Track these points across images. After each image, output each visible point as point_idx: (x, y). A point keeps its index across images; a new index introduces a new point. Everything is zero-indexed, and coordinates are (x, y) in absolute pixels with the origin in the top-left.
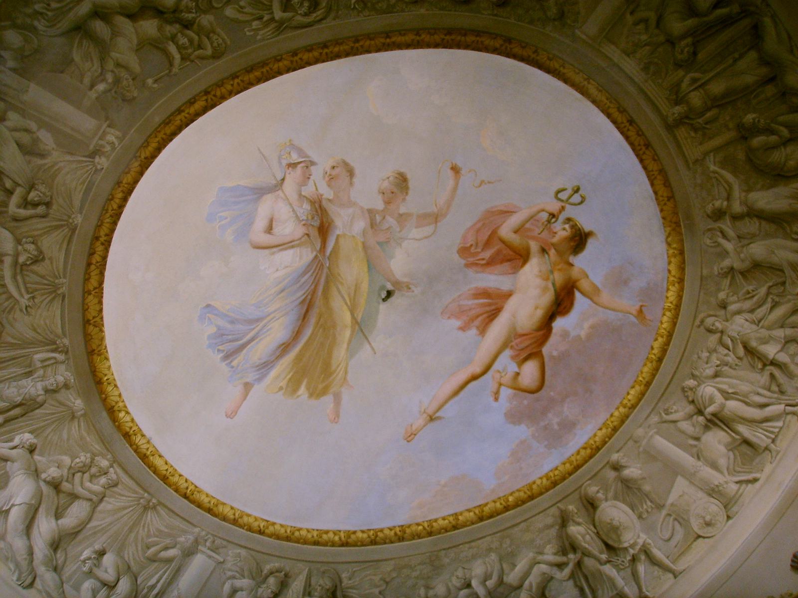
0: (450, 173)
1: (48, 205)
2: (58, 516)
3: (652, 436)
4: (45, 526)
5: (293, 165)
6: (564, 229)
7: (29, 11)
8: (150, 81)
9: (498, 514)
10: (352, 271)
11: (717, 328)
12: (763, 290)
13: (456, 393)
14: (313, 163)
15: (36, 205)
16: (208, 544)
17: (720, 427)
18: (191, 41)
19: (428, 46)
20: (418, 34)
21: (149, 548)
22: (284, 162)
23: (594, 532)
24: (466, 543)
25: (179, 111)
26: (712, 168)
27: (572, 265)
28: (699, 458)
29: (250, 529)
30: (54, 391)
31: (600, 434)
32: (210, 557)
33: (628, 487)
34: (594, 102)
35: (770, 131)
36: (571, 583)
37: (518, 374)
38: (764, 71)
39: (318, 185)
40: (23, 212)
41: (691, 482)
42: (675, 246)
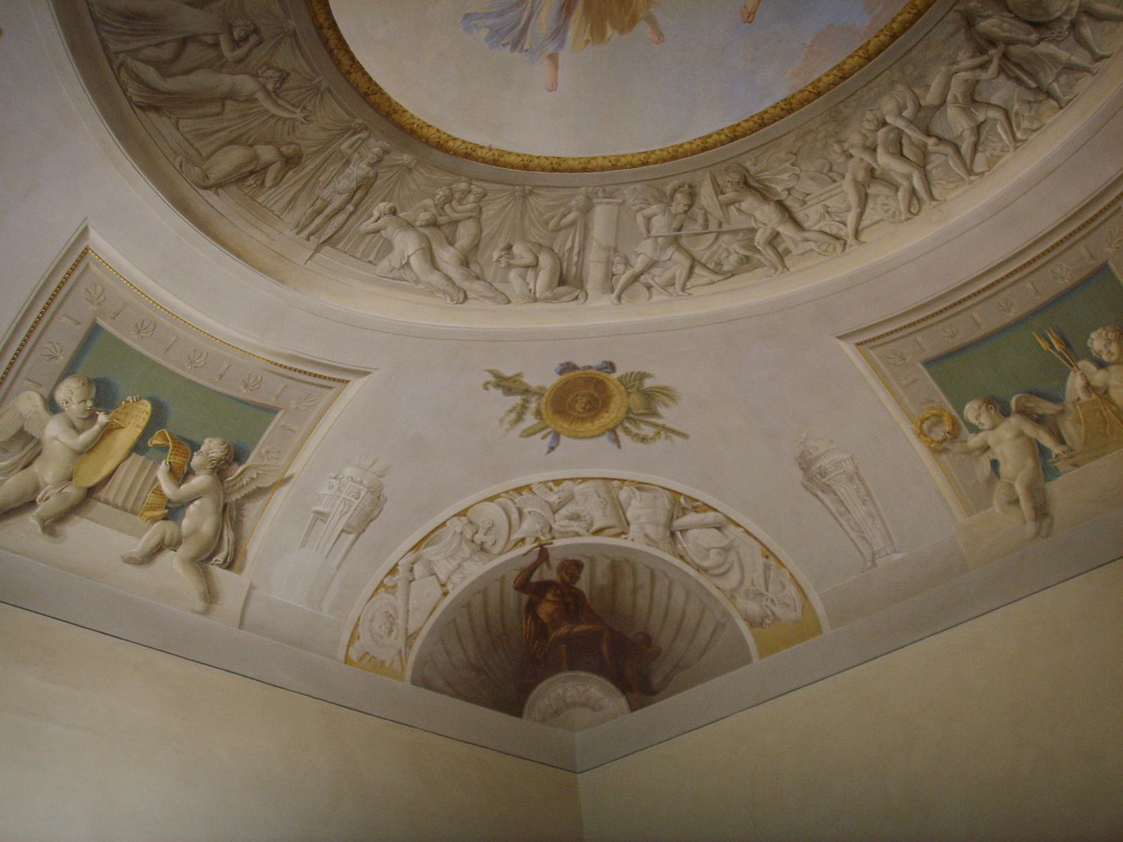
1: (256, 31)
2: (452, 243)
4: (447, 256)
9: (886, 47)
15: (245, 39)
16: (600, 194)
21: (547, 224)
23: (1012, 18)
24: (864, 86)
30: (379, 161)
32: (608, 203)
36: (1002, 78)
40: (240, 52)
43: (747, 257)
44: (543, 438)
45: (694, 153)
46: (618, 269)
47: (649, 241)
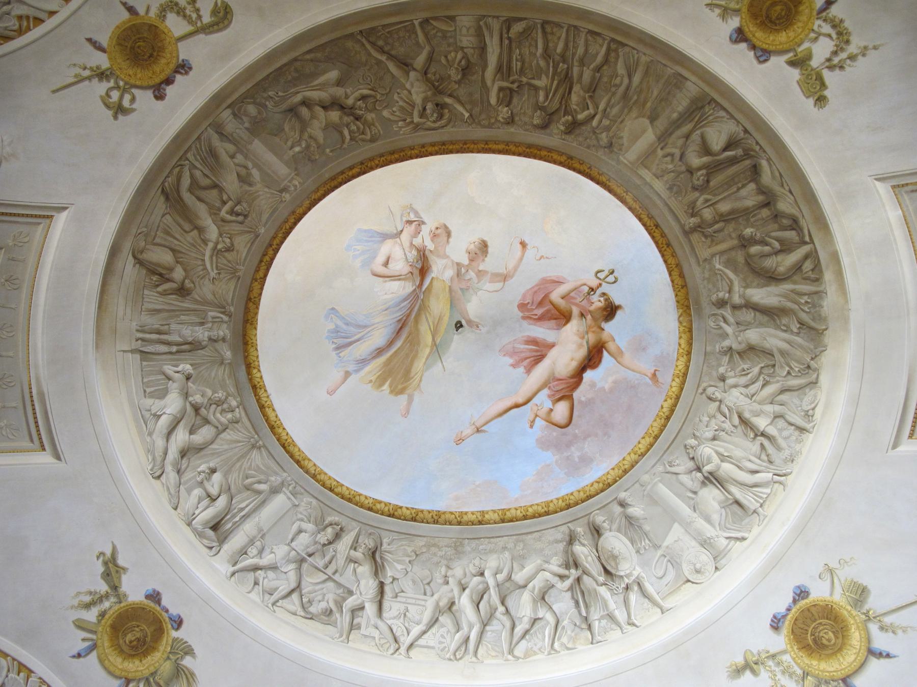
0: (519, 247)
1: (246, 216)
2: (192, 432)
3: (655, 484)
4: (181, 437)
5: (410, 222)
7: (265, 95)
8: (328, 150)
10: (438, 306)
12: (756, 370)
13: (501, 414)
14: (423, 223)
15: (238, 215)
16: (290, 488)
18: (358, 128)
19: (514, 154)
20: (507, 145)
21: (247, 478)
22: (405, 219)
25: (342, 173)
27: (603, 330)
28: (695, 511)
29: (324, 485)
30: (215, 341)
32: (289, 498)
34: (630, 209)
35: (763, 243)
36: (569, 594)
37: (551, 410)
38: (761, 198)
39: (425, 239)
40: (229, 217)
43: (331, 611)
44: (83, 640)
45: (362, 507)
46: (253, 551)
47: (287, 548)
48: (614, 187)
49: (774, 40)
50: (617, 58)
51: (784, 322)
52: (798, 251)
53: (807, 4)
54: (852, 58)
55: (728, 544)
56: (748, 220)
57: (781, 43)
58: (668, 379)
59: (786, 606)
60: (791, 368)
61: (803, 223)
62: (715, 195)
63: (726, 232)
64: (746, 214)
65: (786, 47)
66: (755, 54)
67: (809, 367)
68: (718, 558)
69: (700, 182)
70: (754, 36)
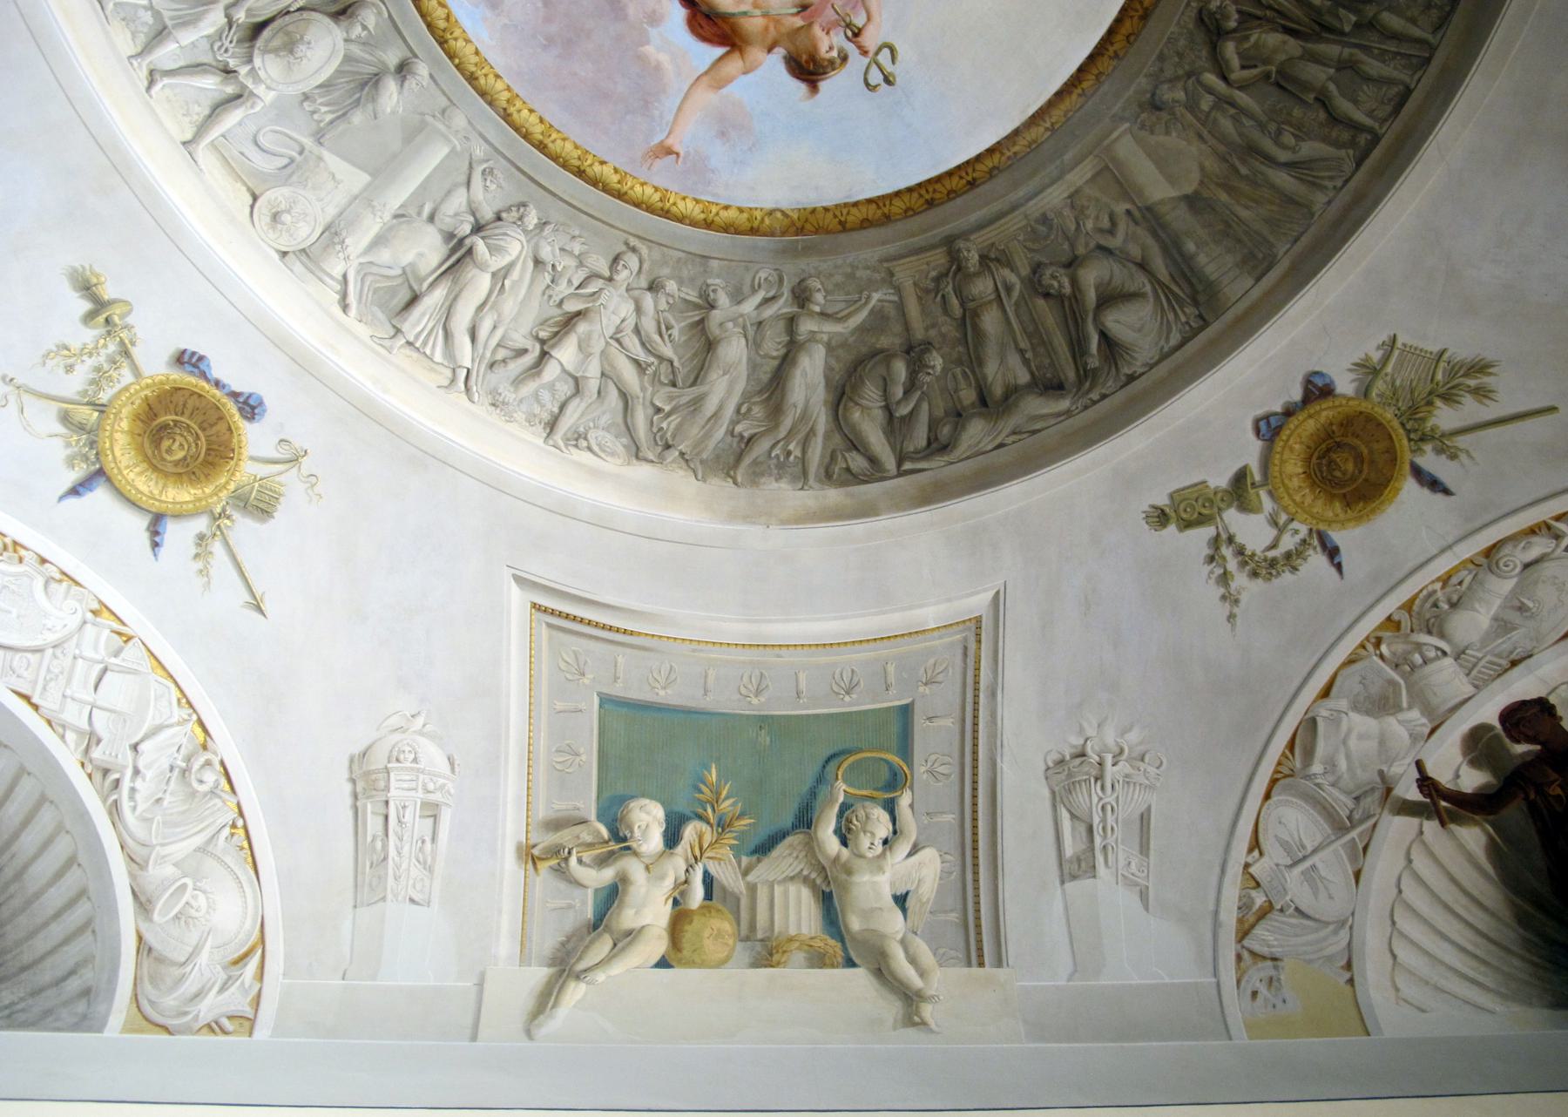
6: (831, 48)
11: (617, 272)
12: (667, 351)
17: (449, 257)
26: (876, 296)
27: (770, 50)
28: (396, 216)
31: (469, 50)
33: (366, 83)
34: (1016, 133)
41: (356, 198)
42: (767, 221)
48: (1067, 103)
49: (1292, 450)
50: (1338, 145)
51: (756, 409)
52: (888, 449)
53: (1342, 516)
54: (1225, 578)
55: (332, 278)
56: (959, 362)
57: (1283, 462)
58: (654, 180)
59: (225, 380)
60: (669, 415)
61: (938, 461)
62: (1017, 304)
63: (942, 319)
64: (971, 358)
65: (1274, 471)
66: (1276, 414)
67: (668, 447)
68: (304, 258)
69: (1046, 280)
70: (1310, 416)
